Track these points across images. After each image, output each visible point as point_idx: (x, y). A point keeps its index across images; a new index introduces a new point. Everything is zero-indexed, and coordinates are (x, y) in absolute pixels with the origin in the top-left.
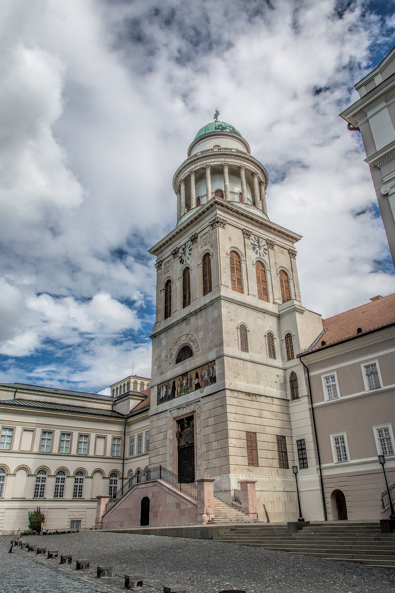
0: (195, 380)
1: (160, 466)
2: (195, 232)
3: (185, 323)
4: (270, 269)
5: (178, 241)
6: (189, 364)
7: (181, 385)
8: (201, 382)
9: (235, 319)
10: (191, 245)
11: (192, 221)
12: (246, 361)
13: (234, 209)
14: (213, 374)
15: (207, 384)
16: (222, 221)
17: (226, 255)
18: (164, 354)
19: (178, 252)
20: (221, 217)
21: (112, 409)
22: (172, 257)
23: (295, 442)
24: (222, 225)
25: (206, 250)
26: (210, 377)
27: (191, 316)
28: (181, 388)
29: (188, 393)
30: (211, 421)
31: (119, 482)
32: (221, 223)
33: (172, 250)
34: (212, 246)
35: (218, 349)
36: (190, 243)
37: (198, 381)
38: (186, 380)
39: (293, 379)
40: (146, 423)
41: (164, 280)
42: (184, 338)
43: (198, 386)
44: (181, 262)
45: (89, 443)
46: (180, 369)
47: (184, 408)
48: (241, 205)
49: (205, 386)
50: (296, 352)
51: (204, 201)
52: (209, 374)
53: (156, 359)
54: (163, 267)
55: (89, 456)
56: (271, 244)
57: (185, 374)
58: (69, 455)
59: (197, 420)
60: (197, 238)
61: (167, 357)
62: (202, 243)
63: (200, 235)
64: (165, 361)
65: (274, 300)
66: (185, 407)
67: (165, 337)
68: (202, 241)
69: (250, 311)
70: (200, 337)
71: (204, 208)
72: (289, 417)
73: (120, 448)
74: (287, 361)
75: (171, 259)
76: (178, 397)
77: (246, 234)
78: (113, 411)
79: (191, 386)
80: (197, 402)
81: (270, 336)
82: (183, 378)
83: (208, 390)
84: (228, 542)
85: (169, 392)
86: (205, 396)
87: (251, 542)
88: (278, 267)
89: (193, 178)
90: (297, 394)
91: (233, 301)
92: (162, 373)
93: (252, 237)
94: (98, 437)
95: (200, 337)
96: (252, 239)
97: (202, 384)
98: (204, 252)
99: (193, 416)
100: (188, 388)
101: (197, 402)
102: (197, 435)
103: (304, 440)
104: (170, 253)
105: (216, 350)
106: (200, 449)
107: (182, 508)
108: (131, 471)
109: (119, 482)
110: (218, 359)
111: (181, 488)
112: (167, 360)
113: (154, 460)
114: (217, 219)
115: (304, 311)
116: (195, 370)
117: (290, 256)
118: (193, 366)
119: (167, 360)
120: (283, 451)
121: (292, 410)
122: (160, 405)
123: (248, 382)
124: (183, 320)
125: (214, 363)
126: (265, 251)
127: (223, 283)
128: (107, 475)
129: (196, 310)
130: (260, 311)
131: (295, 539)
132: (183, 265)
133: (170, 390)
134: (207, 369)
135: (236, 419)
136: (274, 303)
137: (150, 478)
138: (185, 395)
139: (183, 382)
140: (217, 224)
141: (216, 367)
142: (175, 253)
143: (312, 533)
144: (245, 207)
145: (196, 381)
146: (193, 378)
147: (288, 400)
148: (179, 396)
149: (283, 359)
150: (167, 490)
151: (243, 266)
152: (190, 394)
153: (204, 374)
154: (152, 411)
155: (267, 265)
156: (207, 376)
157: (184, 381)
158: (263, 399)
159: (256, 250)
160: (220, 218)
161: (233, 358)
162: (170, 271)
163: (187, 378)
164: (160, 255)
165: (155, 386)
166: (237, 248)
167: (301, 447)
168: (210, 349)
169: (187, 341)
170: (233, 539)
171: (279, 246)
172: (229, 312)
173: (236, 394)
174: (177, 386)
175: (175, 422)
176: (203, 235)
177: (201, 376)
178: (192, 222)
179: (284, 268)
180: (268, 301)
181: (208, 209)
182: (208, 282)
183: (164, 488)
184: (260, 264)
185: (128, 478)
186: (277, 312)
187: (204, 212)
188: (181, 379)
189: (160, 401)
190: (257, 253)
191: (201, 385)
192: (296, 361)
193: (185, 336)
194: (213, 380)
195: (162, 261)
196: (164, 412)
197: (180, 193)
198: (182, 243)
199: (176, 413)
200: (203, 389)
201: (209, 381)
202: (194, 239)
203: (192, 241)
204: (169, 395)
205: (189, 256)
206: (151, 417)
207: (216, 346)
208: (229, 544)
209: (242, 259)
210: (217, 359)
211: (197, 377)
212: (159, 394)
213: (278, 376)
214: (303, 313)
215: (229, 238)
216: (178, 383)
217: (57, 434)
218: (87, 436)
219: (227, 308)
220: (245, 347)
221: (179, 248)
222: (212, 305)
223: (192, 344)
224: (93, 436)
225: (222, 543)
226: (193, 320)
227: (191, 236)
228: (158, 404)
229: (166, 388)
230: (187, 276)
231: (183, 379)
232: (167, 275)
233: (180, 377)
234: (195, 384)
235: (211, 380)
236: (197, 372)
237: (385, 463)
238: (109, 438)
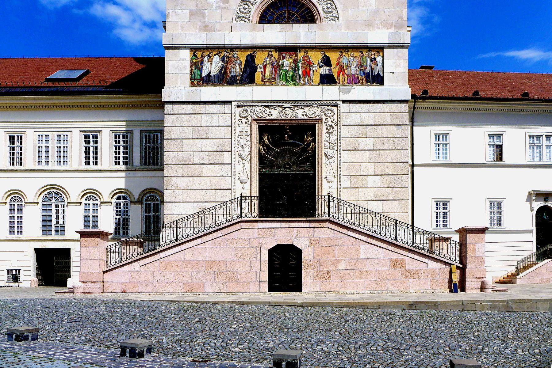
0: (320, 67)
7: (276, 67)
8: (338, 75)
14: (372, 70)
15: (354, 81)
26: (364, 73)
28: (276, 71)
38: (291, 60)
43: (328, 80)
47: (285, 108)
52: (360, 66)
66: (289, 108)
76: (266, 85)
85: (233, 70)
100: (297, 76)
138: (288, 85)
145: (325, 70)
153: (348, 62)
156: (354, 69)
157: (287, 63)
168: (369, 25)
174: (261, 66)
177: (338, 64)
191: (339, 80)
207: (387, 26)
211: (327, 62)
212: (196, 65)
229: (223, 60)
234: (321, 75)
236: (326, 56)
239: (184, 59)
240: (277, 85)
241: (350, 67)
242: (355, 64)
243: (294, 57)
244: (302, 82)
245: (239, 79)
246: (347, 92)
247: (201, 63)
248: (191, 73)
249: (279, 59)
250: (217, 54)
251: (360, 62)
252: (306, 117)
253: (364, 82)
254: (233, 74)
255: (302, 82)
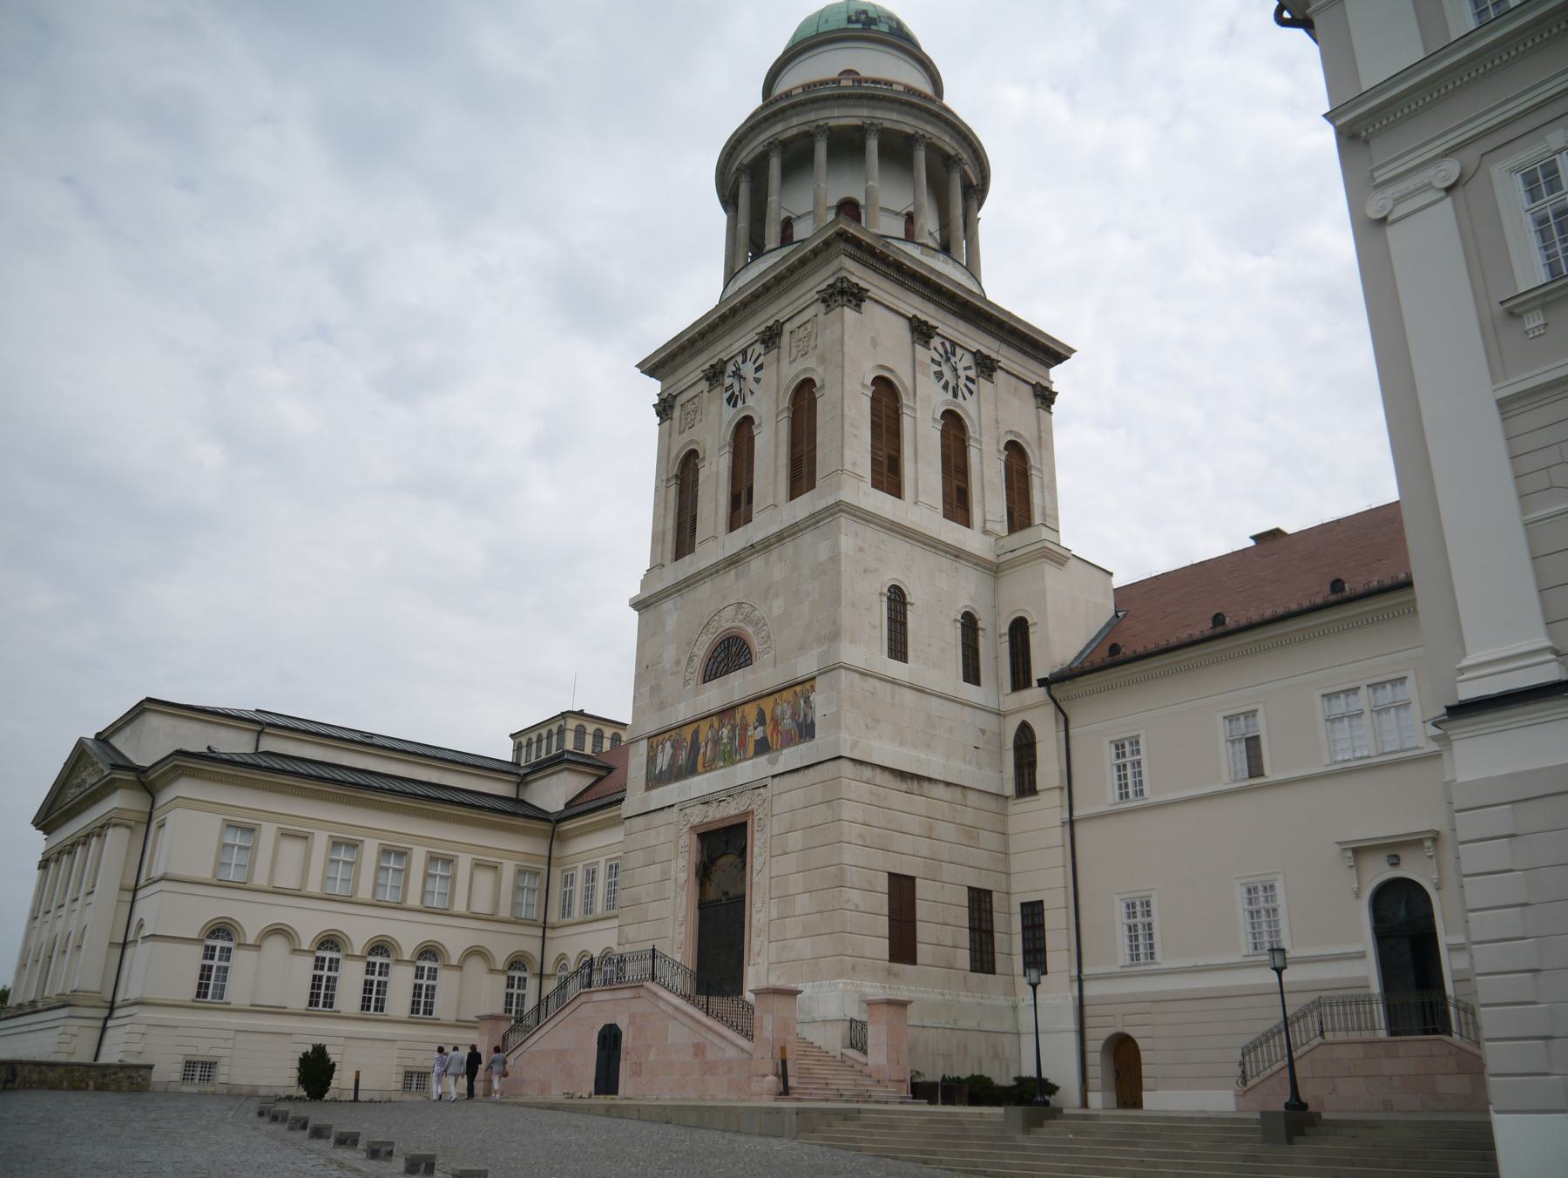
0: (755, 728)
1: (654, 950)
2: (776, 318)
3: (733, 572)
4: (981, 435)
5: (725, 342)
6: (737, 686)
7: (717, 741)
8: (772, 737)
9: (876, 570)
10: (760, 355)
11: (768, 285)
12: (900, 685)
13: (891, 259)
14: (805, 715)
15: (789, 741)
16: (856, 291)
17: (859, 387)
18: (670, 654)
19: (722, 372)
20: (854, 280)
21: (517, 795)
22: (704, 385)
23: (1017, 909)
24: (854, 302)
25: (806, 370)
26: (798, 724)
27: (753, 554)
29: (733, 763)
30: (795, 840)
31: (532, 984)
32: (853, 294)
33: (707, 366)
34: (822, 360)
35: (824, 648)
36: (759, 348)
37: (764, 731)
38: (729, 727)
39: (1024, 742)
40: (615, 836)
41: (679, 447)
42: (729, 613)
43: (763, 747)
44: (729, 401)
45: (452, 879)
46: (716, 695)
48: (909, 248)
49: (783, 747)
50: (1039, 670)
51: (802, 230)
52: (794, 715)
53: (647, 667)
54: (677, 413)
55: (454, 913)
56: (986, 366)
57: (727, 712)
58: (399, 907)
59: (757, 835)
60: (779, 334)
61: (678, 662)
62: (794, 350)
63: (788, 327)
64: (672, 674)
65: (985, 523)
67: (676, 609)
68: (793, 344)
69: (918, 552)
70: (776, 612)
71: (806, 250)
72: (1006, 844)
73: (536, 899)
74: (1010, 691)
75: (702, 392)
76: (706, 772)
77: (922, 332)
78: (518, 801)
79: (743, 743)
80: (759, 788)
81: (969, 624)
82: (720, 721)
83: (791, 757)
84: (840, 1148)
86: (783, 774)
87: (903, 1151)
88: (1002, 431)
89: (775, 165)
90: (1033, 782)
91: (874, 520)
92: (662, 706)
93: (936, 342)
94: (478, 865)
95: (776, 612)
96: (935, 349)
97: (775, 740)
98: (797, 376)
99: (745, 824)
100: (734, 749)
101: (759, 788)
102: (754, 875)
103: (1041, 902)
104: (698, 374)
105: (820, 650)
106: (760, 911)
107: (710, 1056)
108: (563, 957)
109: (532, 984)
110: (823, 676)
111: (708, 1008)
112: (677, 672)
113: (631, 932)
114: (842, 282)
115: (1068, 558)
116: (757, 702)
117: (1037, 404)
118: (752, 691)
119: (677, 672)
120: (984, 927)
121: (1013, 826)
122: (654, 792)
123: (902, 743)
124: (729, 565)
125: (812, 687)
126: (969, 384)
127: (848, 466)
128: (500, 964)
129: (768, 537)
130: (947, 553)
131: (1024, 1148)
132: (735, 410)
133: (683, 753)
134: (790, 702)
135: (864, 840)
136: (985, 532)
137: (624, 978)
139: (722, 733)
140: (839, 298)
141: (817, 698)
142: (714, 375)
143: (1071, 1136)
144: (922, 253)
145: (758, 733)
146: (751, 722)
147: (1007, 797)
148: (709, 768)
149: (999, 686)
150: (670, 1011)
151: (906, 423)
152: (740, 765)
154: (627, 808)
155: (973, 424)
156: (788, 721)
157: (725, 731)
158: (939, 791)
159: (943, 381)
160: (849, 281)
161: (866, 675)
162: (698, 426)
163: (732, 722)
164: (671, 380)
165: (643, 739)
166: (891, 371)
167: (1033, 920)
168: (802, 648)
169: (737, 624)
170: (854, 1140)
171: (1008, 372)
172: (861, 550)
173: (867, 773)
174: (703, 744)
175: (695, 837)
176: (799, 328)
177: (772, 718)
178: (766, 288)
179: (1019, 435)
180: (967, 523)
181: (815, 253)
182: (805, 463)
183: (661, 1005)
184: (953, 424)
185: (555, 975)
186: (991, 557)
187: (803, 262)
188: (716, 725)
189: (655, 780)
190: (945, 387)
192: (1036, 694)
193: (731, 607)
194: (806, 731)
195: (676, 396)
196: (666, 810)
197: (736, 206)
198: (735, 347)
199: (698, 816)
200: (778, 753)
201: (795, 731)
202: (771, 337)
203: (763, 342)
204: (680, 766)
205: (753, 385)
206: (627, 822)
208: (843, 1153)
209: (904, 401)
210: (820, 674)
211: (761, 720)
212: (651, 760)
213: (983, 732)
214: (1062, 565)
215: (873, 340)
216: (705, 732)
217: (371, 849)
218: (449, 861)
219: (856, 536)
220: (898, 649)
221: (725, 363)
222: (813, 527)
223: (750, 630)
224: (464, 863)
225: (825, 1149)
226: (756, 564)
227: (762, 328)
228: (648, 789)
229: (673, 746)
230: (745, 440)
231: (722, 725)
232: (686, 437)
233: (714, 718)
235: (800, 731)
237: (1285, 968)
238: (508, 869)
239: (642, 755)
240: (716, 769)
241: (784, 719)
242: (789, 713)
243: (732, 722)
244: (738, 757)
245: (684, 769)
246: (773, 762)
247: (656, 755)
248: (647, 773)
249: (720, 729)
250: (669, 739)
251: (793, 709)
252: (737, 812)
253: (797, 740)
254: (680, 763)
255: (738, 757)
